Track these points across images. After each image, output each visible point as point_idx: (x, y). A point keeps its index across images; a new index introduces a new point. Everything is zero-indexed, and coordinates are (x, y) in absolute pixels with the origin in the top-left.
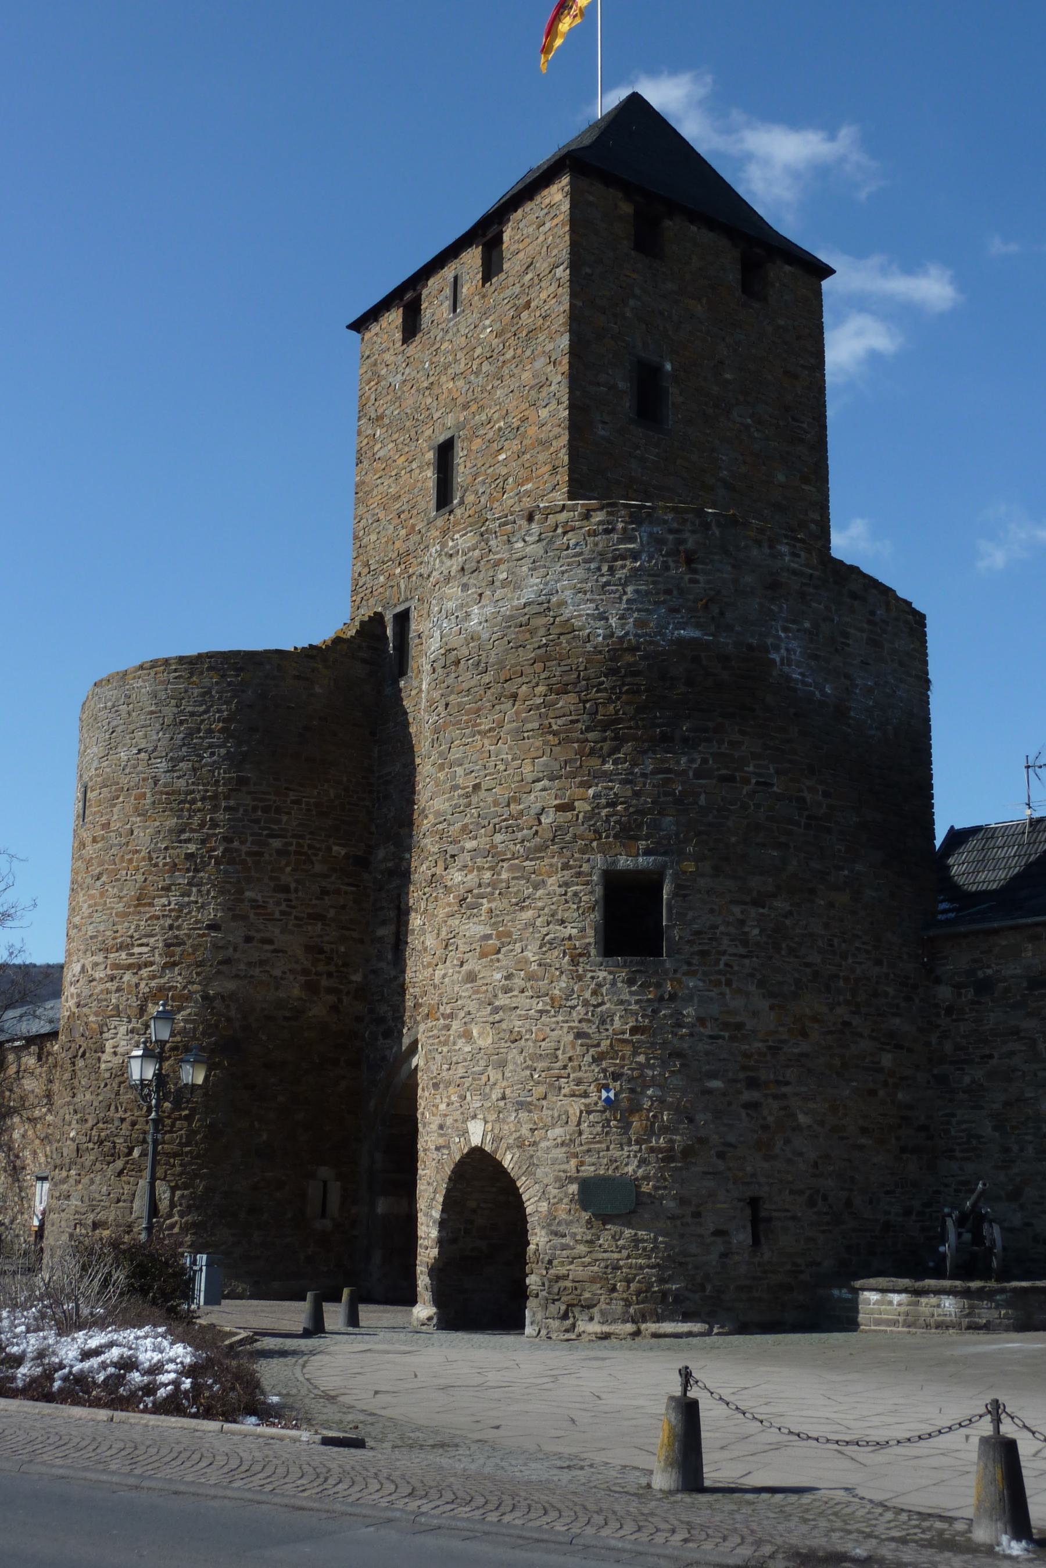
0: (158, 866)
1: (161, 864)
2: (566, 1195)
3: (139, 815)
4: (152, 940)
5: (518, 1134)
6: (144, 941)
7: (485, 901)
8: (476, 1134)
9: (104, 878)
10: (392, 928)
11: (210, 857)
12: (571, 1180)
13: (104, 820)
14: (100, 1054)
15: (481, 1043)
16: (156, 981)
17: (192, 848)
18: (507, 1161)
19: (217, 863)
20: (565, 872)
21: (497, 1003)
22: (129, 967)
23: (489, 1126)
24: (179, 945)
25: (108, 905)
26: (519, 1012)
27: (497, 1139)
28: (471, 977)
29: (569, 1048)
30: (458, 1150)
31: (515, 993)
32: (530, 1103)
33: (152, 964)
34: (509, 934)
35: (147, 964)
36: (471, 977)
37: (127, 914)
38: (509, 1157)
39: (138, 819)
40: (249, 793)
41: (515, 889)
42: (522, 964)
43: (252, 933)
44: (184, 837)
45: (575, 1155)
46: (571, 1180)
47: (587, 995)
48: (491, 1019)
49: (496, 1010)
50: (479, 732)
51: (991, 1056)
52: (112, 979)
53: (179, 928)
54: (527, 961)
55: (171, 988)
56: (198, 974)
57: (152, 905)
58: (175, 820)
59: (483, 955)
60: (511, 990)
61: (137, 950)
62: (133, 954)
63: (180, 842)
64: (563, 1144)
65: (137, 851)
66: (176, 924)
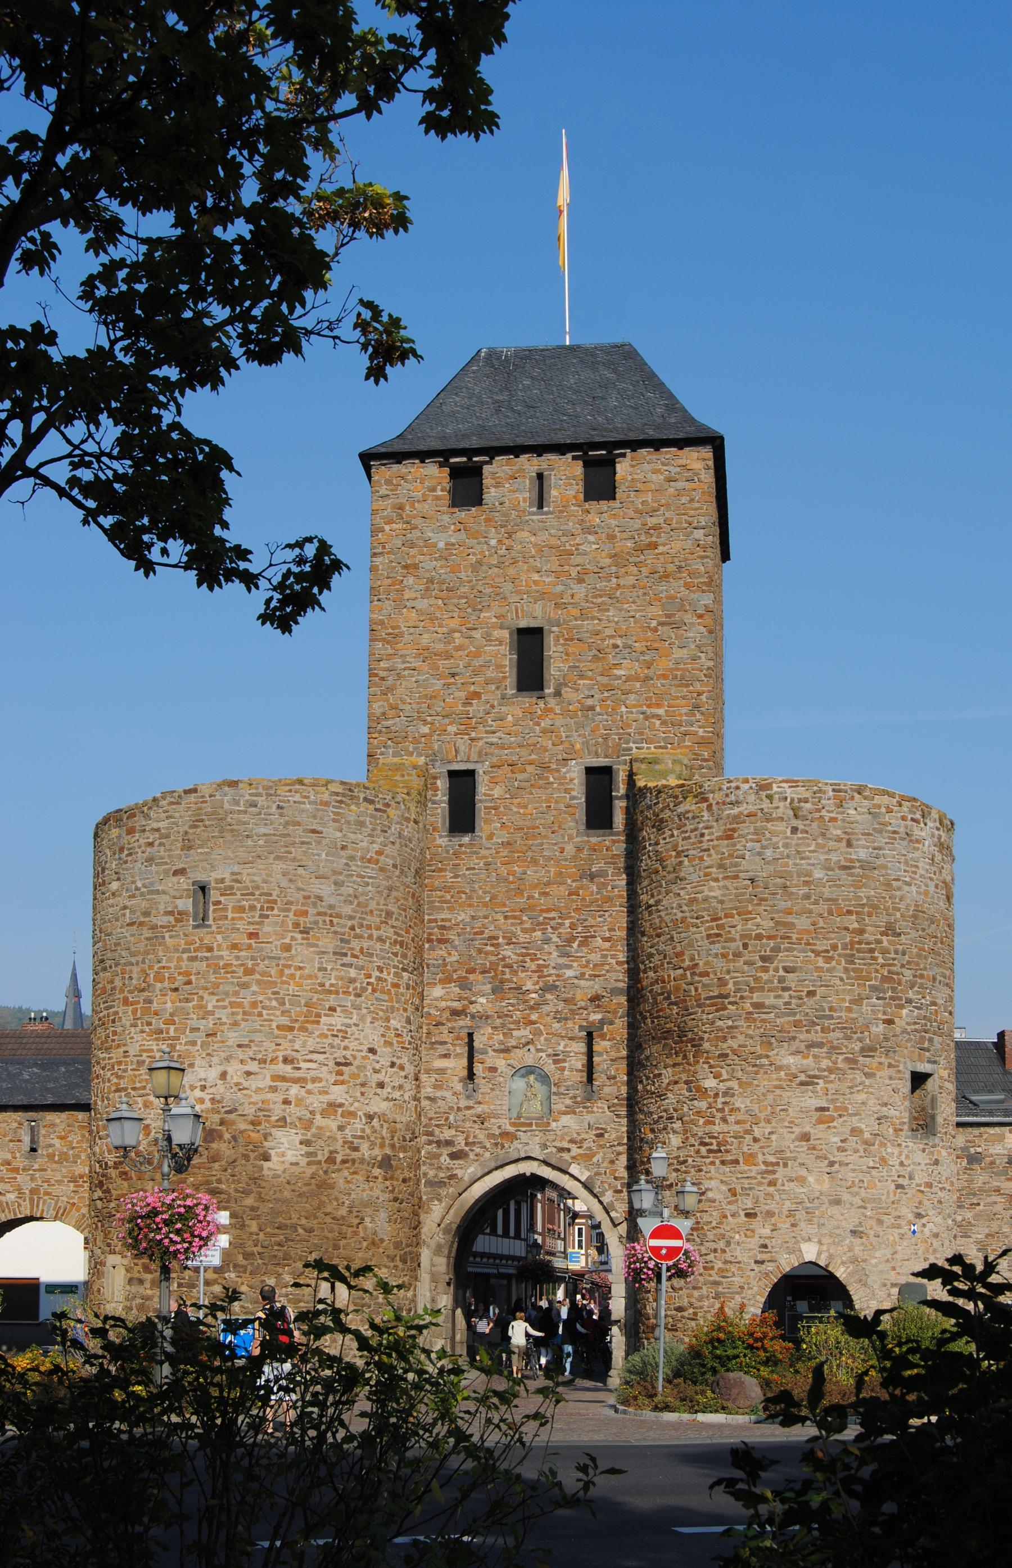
0: (324, 985)
1: (327, 985)
2: (889, 1295)
3: (301, 932)
4: (321, 1057)
5: (851, 1254)
6: (315, 1057)
7: (820, 1081)
8: (810, 1252)
9: (254, 988)
10: (464, 1062)
11: (368, 984)
12: (893, 1285)
13: (251, 929)
14: (262, 1162)
15: (817, 1187)
16: (327, 1097)
17: (353, 973)
18: (840, 1273)
19: (374, 991)
20: (891, 1069)
21: (832, 1159)
22: (296, 1081)
23: (825, 1248)
24: (346, 1064)
25: (266, 1017)
26: (851, 1166)
27: (831, 1257)
28: (805, 1137)
29: (892, 1195)
30: (787, 1263)
31: (849, 1153)
32: (862, 1232)
33: (320, 1080)
34: (846, 1109)
35: (314, 1080)
36: (805, 1137)
37: (291, 1029)
38: (842, 1269)
39: (299, 936)
40: (393, 927)
41: (851, 1076)
42: (855, 1131)
43: (395, 1059)
44: (347, 960)
45: (894, 1269)
46: (893, 1285)
47: (903, 1158)
48: (828, 1170)
49: (832, 1164)
50: (813, 951)
51: (978, 1204)
52: (274, 1089)
53: (346, 1048)
54: (861, 1131)
55: (341, 1105)
56: (363, 1094)
57: (318, 1022)
58: (339, 943)
59: (820, 1121)
60: (846, 1150)
61: (303, 1065)
62: (299, 1069)
63: (343, 965)
64: (887, 1261)
65: (300, 968)
66: (343, 1044)
